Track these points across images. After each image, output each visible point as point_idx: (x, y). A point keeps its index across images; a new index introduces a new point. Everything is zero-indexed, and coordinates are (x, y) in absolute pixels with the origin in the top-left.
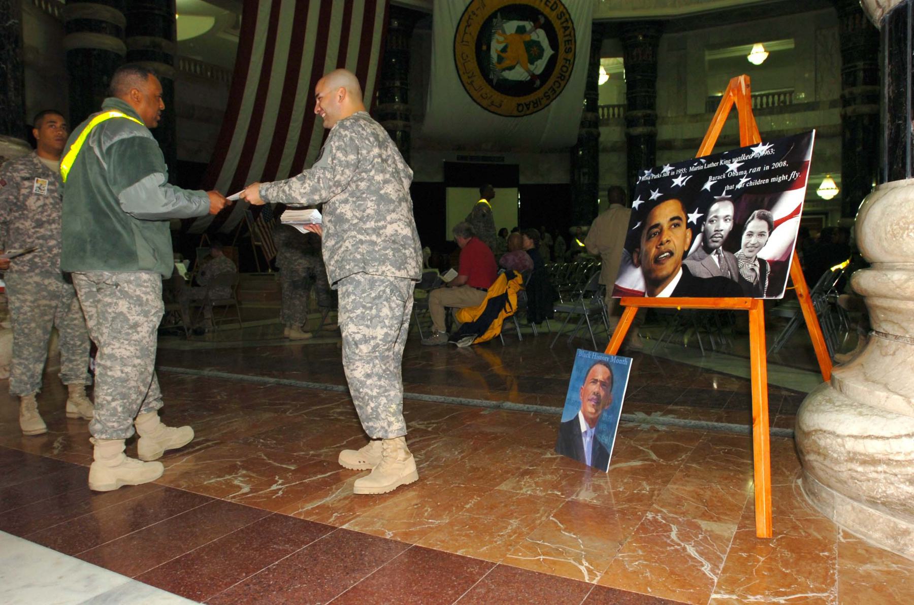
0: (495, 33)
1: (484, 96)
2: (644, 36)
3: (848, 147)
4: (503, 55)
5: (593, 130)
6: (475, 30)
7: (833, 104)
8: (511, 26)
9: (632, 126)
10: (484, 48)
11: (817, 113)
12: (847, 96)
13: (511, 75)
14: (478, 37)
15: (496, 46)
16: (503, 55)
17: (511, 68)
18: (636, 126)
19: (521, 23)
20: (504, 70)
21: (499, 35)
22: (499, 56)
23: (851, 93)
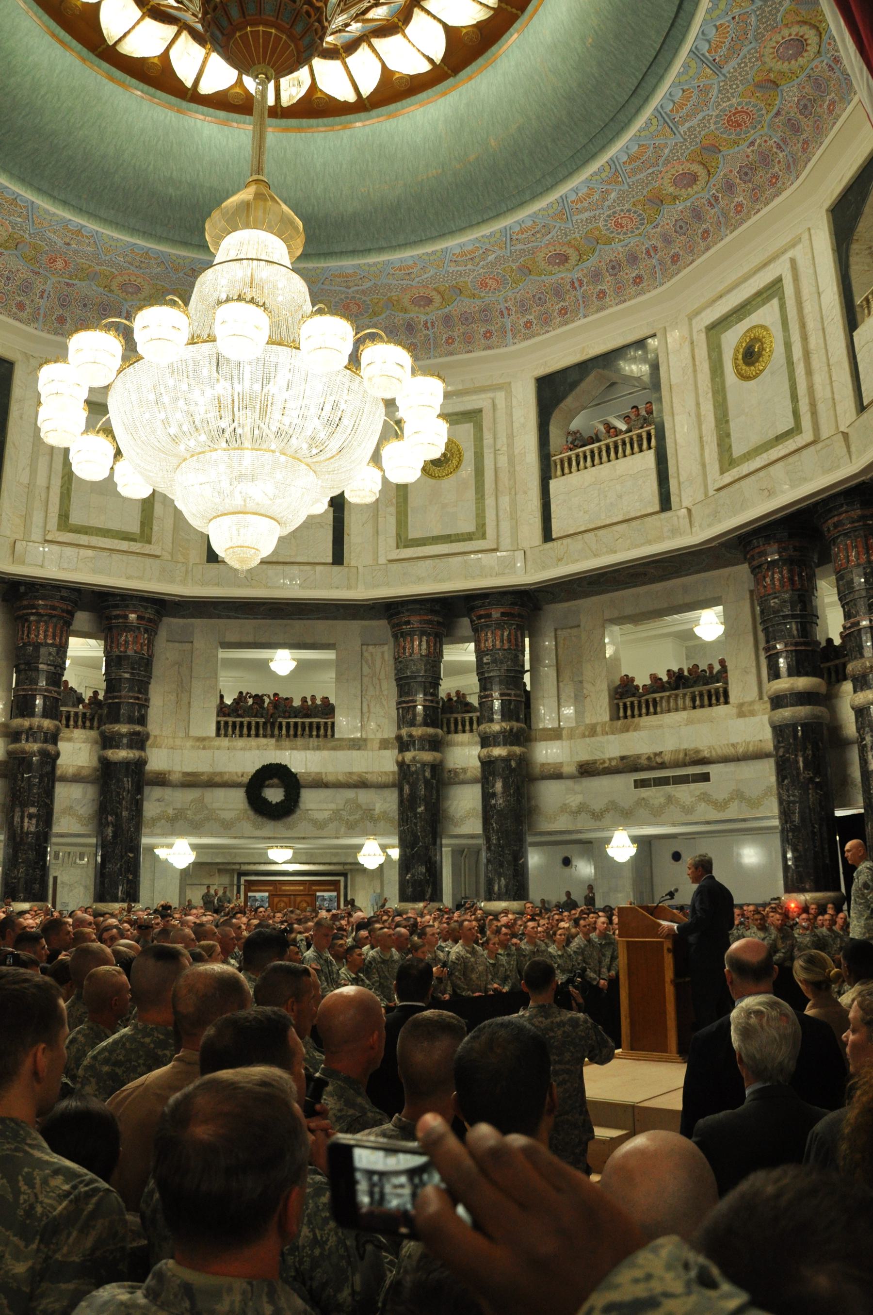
2: (139, 618)
3: (406, 806)
5: (50, 747)
7: (384, 744)
9: (111, 747)
11: (364, 753)
12: (405, 738)
18: (118, 747)
23: (410, 736)
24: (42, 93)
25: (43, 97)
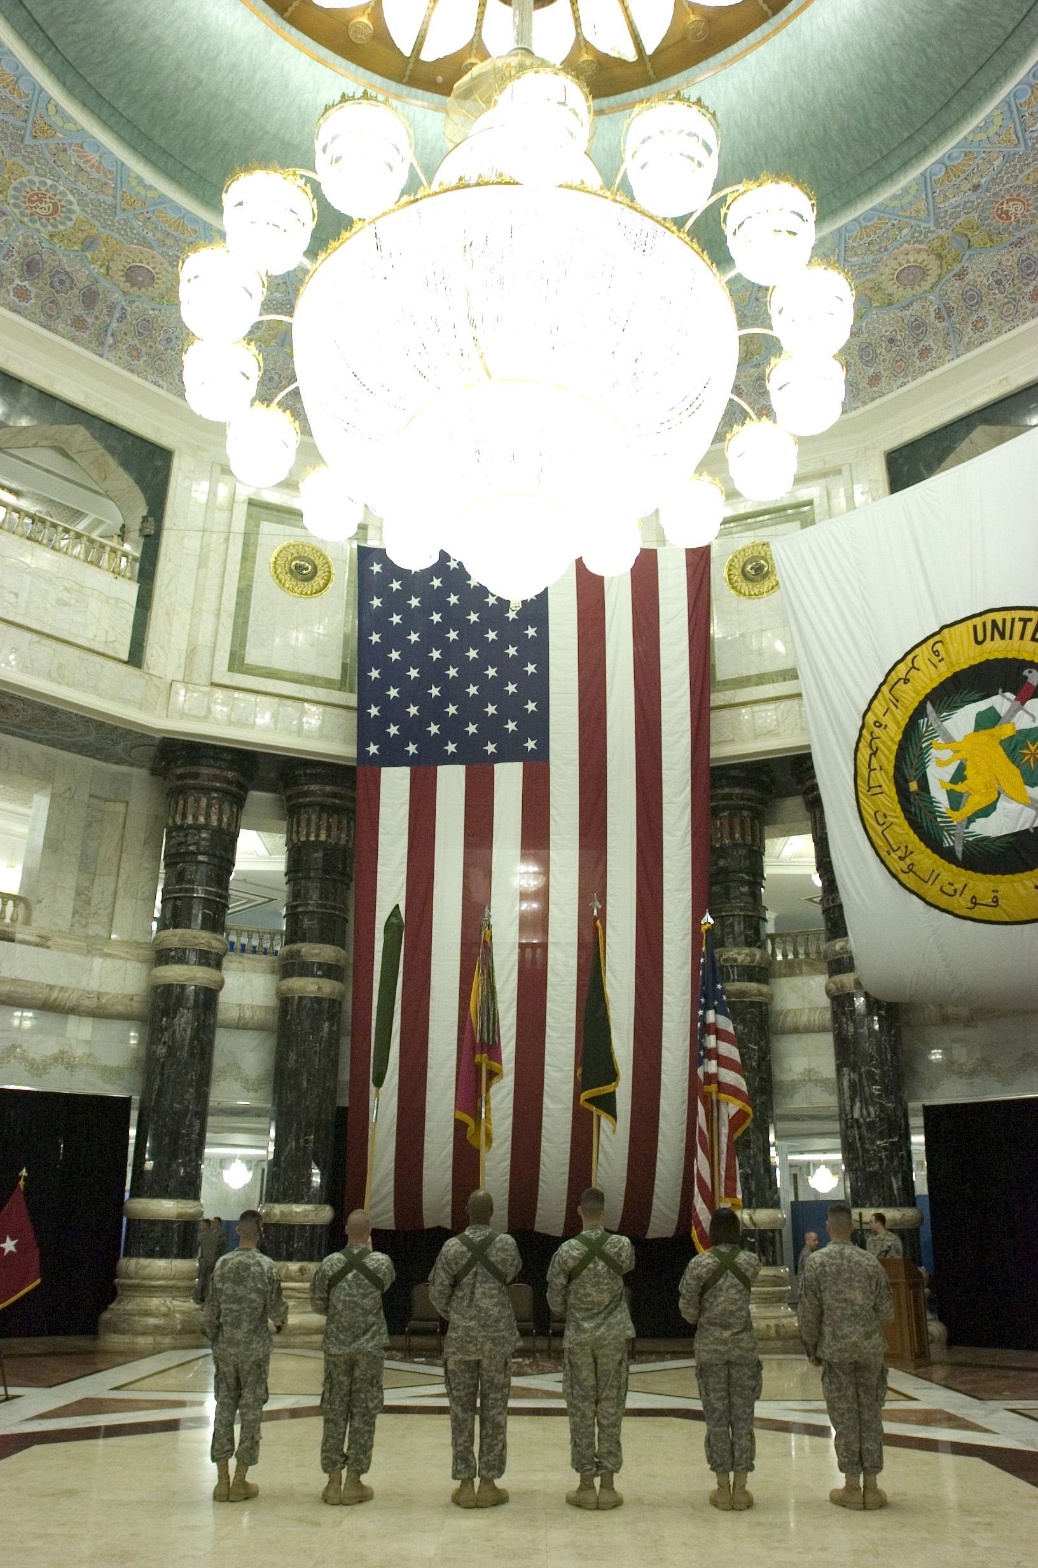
0: (929, 747)
1: (947, 889)
4: (960, 788)
6: (887, 757)
8: (962, 720)
10: (913, 786)
13: (991, 827)
14: (896, 767)
15: (938, 776)
16: (960, 788)
17: (987, 811)
19: (983, 705)
20: (971, 820)
21: (939, 749)
22: (951, 794)
24: (755, 124)
25: (759, 125)
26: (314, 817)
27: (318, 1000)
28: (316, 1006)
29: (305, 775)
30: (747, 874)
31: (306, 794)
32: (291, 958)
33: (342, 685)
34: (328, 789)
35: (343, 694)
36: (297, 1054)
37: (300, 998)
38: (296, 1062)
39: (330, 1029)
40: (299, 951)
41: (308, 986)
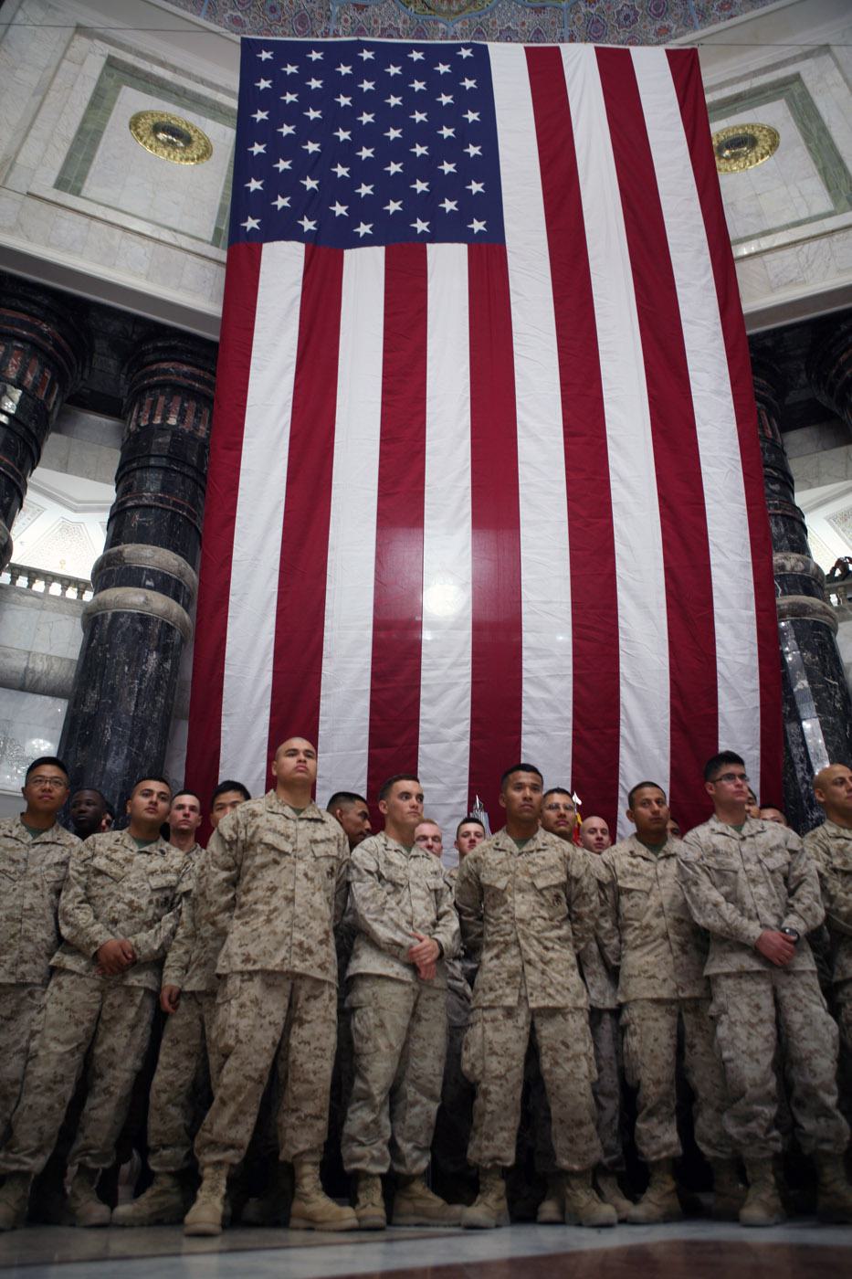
26: (162, 399)
27: (144, 619)
28: (140, 628)
29: (156, 349)
30: (775, 469)
31: (154, 373)
32: (109, 565)
33: (215, 243)
34: (185, 368)
35: (214, 248)
36: (101, 693)
37: (116, 616)
38: (98, 703)
39: (160, 664)
40: (120, 552)
41: (134, 598)
